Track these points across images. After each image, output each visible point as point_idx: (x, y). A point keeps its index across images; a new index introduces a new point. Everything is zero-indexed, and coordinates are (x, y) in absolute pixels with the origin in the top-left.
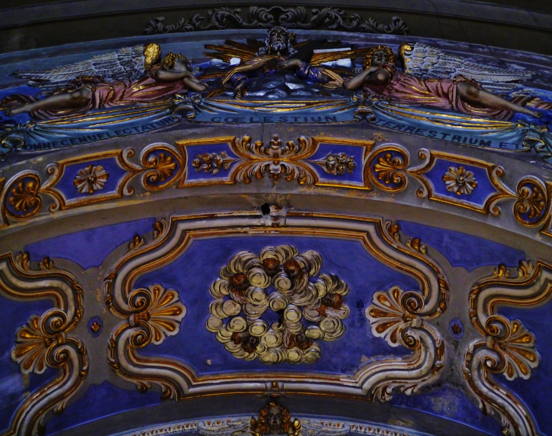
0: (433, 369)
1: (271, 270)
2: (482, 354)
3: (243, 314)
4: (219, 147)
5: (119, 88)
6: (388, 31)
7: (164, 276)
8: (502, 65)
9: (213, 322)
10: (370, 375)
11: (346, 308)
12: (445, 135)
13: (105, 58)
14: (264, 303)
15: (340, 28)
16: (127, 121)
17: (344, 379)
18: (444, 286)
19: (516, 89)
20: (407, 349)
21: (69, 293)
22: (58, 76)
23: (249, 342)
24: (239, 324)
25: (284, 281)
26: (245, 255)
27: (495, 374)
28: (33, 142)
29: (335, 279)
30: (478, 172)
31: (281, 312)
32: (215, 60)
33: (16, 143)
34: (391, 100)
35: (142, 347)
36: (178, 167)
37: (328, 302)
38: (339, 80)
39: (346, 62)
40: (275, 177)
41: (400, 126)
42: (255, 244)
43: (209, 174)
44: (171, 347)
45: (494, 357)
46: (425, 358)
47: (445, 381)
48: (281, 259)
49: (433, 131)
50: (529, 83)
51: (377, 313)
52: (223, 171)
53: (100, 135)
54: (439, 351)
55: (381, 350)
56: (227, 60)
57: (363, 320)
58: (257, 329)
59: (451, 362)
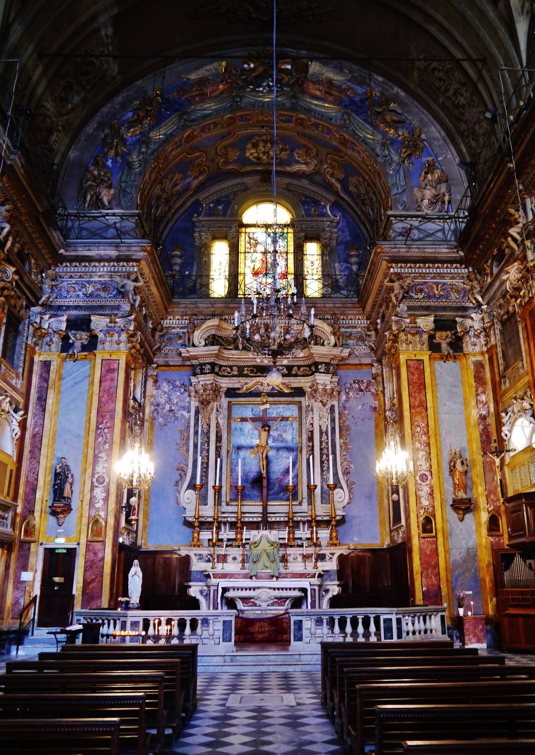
0: (314, 169)
1: (265, 142)
2: (328, 169)
3: (256, 152)
4: (249, 115)
5: (215, 87)
6: (304, 49)
7: (233, 145)
8: (340, 70)
9: (248, 154)
10: (296, 168)
11: (288, 152)
12: (319, 114)
13: (208, 67)
14: (263, 150)
15: (288, 47)
16: (219, 106)
17: (288, 168)
18: (318, 151)
19: (345, 83)
20: (307, 164)
21: (204, 155)
22: (193, 76)
23: (259, 158)
24: (256, 155)
25: (269, 145)
26: (257, 138)
27: (332, 175)
28: (191, 118)
29: (285, 144)
30: (328, 128)
31: (268, 152)
32: (246, 66)
33: (185, 120)
34: (304, 92)
35: (226, 163)
36: (236, 120)
37: (282, 150)
38: (286, 79)
39: (289, 67)
40: (266, 122)
41: (305, 109)
42: (260, 135)
43: (245, 121)
44: (235, 161)
45: (331, 171)
46: (312, 167)
47: (317, 172)
48: (268, 138)
49: (315, 111)
50: (349, 81)
51: (297, 153)
52: (249, 120)
53: (210, 114)
54: (316, 166)
55: (298, 162)
56: (249, 65)
57: (293, 155)
58: (261, 156)
59: (319, 169)
